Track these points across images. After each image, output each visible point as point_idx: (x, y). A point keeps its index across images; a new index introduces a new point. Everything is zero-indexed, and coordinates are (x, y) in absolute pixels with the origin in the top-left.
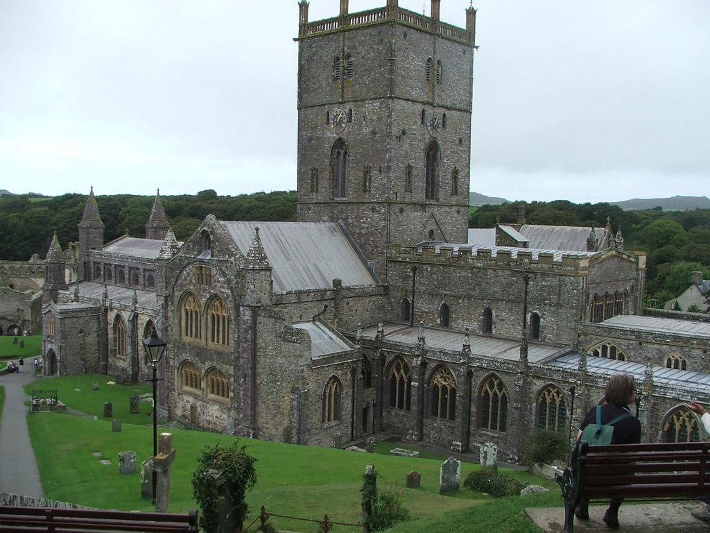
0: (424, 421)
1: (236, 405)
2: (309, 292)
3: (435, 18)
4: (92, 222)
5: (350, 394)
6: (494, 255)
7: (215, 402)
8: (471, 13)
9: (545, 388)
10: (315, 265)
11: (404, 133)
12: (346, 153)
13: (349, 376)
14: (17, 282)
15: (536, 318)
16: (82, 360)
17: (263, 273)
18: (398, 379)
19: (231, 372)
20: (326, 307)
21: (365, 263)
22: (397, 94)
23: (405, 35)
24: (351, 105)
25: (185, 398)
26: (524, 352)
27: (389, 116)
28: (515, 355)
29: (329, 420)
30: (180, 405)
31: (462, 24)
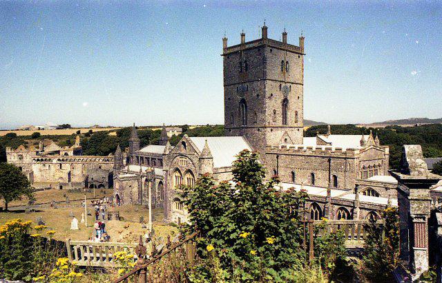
3: (285, 43)
4: (134, 139)
6: (314, 149)
8: (302, 39)
9: (339, 208)
11: (272, 95)
12: (246, 105)
15: (335, 177)
22: (268, 78)
23: (271, 50)
24: (247, 84)
25: (176, 214)
26: (329, 192)
27: (265, 88)
28: (325, 194)
30: (174, 217)
31: (297, 44)
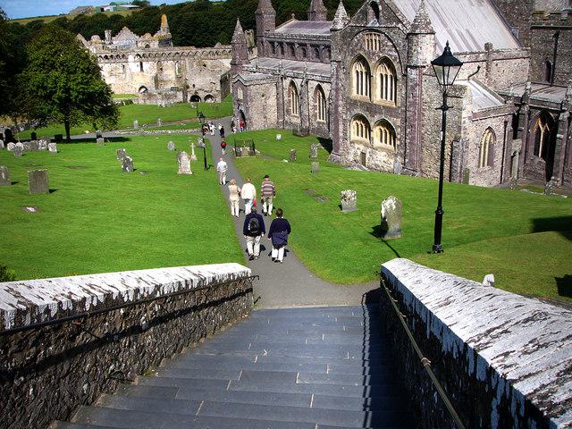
0: (566, 169)
1: (402, 152)
2: (466, 54)
5: (502, 143)
7: (382, 149)
10: (468, 31)
13: (502, 126)
14: (209, 63)
16: (265, 117)
17: (428, 36)
18: (543, 131)
19: (399, 123)
20: (479, 68)
21: (510, 29)
25: (356, 146)
29: (483, 166)
30: (352, 151)
